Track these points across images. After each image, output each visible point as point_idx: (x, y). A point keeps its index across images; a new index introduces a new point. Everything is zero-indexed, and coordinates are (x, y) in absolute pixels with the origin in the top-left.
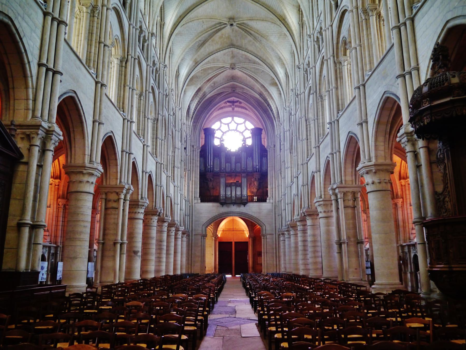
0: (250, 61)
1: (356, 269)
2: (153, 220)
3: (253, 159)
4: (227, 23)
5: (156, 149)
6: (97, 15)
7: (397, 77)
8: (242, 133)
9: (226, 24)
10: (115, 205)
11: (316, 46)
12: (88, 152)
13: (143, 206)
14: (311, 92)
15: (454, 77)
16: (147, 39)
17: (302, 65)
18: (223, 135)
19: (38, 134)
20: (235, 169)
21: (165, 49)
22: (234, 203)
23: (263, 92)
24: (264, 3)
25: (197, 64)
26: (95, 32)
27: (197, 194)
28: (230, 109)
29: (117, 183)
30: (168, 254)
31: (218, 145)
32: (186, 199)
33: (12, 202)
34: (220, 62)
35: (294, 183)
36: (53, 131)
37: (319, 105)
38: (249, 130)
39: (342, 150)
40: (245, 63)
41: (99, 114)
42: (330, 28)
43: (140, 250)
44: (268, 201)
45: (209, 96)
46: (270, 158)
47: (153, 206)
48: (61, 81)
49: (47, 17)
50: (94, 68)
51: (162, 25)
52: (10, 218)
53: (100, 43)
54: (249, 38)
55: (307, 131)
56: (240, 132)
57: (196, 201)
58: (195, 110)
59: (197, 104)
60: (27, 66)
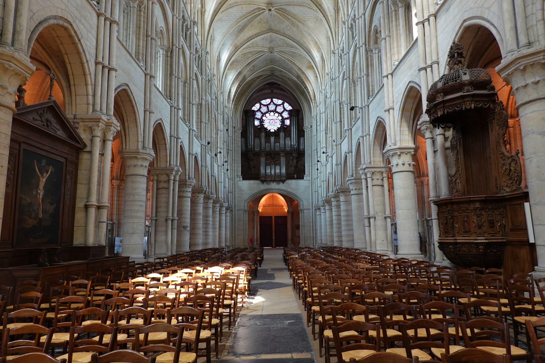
0: (288, 45)
1: (383, 241)
2: (199, 198)
3: (291, 138)
5: (201, 132)
6: (143, 10)
7: (420, 70)
8: (280, 114)
9: (264, 9)
10: (165, 185)
11: (350, 33)
12: (141, 139)
13: (191, 185)
14: (345, 77)
15: (465, 74)
16: (189, 27)
17: (337, 50)
18: (262, 116)
19: (98, 126)
20: (274, 149)
21: (206, 36)
22: (274, 181)
23: (301, 75)
25: (236, 48)
26: (142, 26)
27: (239, 172)
28: (269, 91)
30: (214, 228)
31: (259, 126)
32: (229, 177)
33: (79, 186)
34: (259, 47)
35: (329, 162)
36: (112, 123)
37: (352, 90)
38: (287, 111)
39: (371, 133)
40: (283, 47)
41: (150, 104)
42: (363, 16)
43: (189, 225)
44: (305, 178)
45: (248, 79)
46: (307, 138)
47: (199, 185)
48: (116, 77)
49: (100, 17)
50: (143, 61)
51: (203, 13)
52: (78, 200)
53: (147, 36)
55: (341, 114)
57: (238, 179)
58: (236, 93)
59: (238, 87)
60: (86, 65)
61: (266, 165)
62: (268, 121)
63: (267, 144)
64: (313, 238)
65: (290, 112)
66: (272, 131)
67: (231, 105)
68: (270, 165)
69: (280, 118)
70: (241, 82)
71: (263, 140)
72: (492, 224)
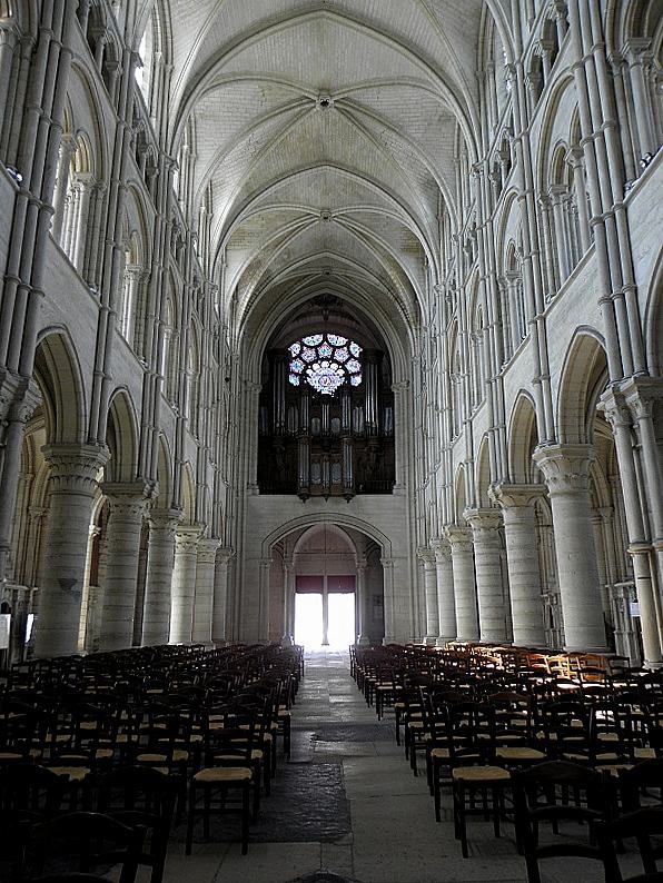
2: (131, 509)
4: (316, 98)
5: (145, 343)
8: (342, 365)
18: (306, 368)
21: (172, 124)
22: (327, 496)
24: (396, 35)
27: (252, 477)
28: (321, 318)
37: (541, 221)
40: (350, 205)
44: (394, 491)
54: (362, 138)
55: (499, 307)
57: (251, 491)
64: (414, 624)
65: (362, 359)
67: (237, 331)
69: (341, 372)
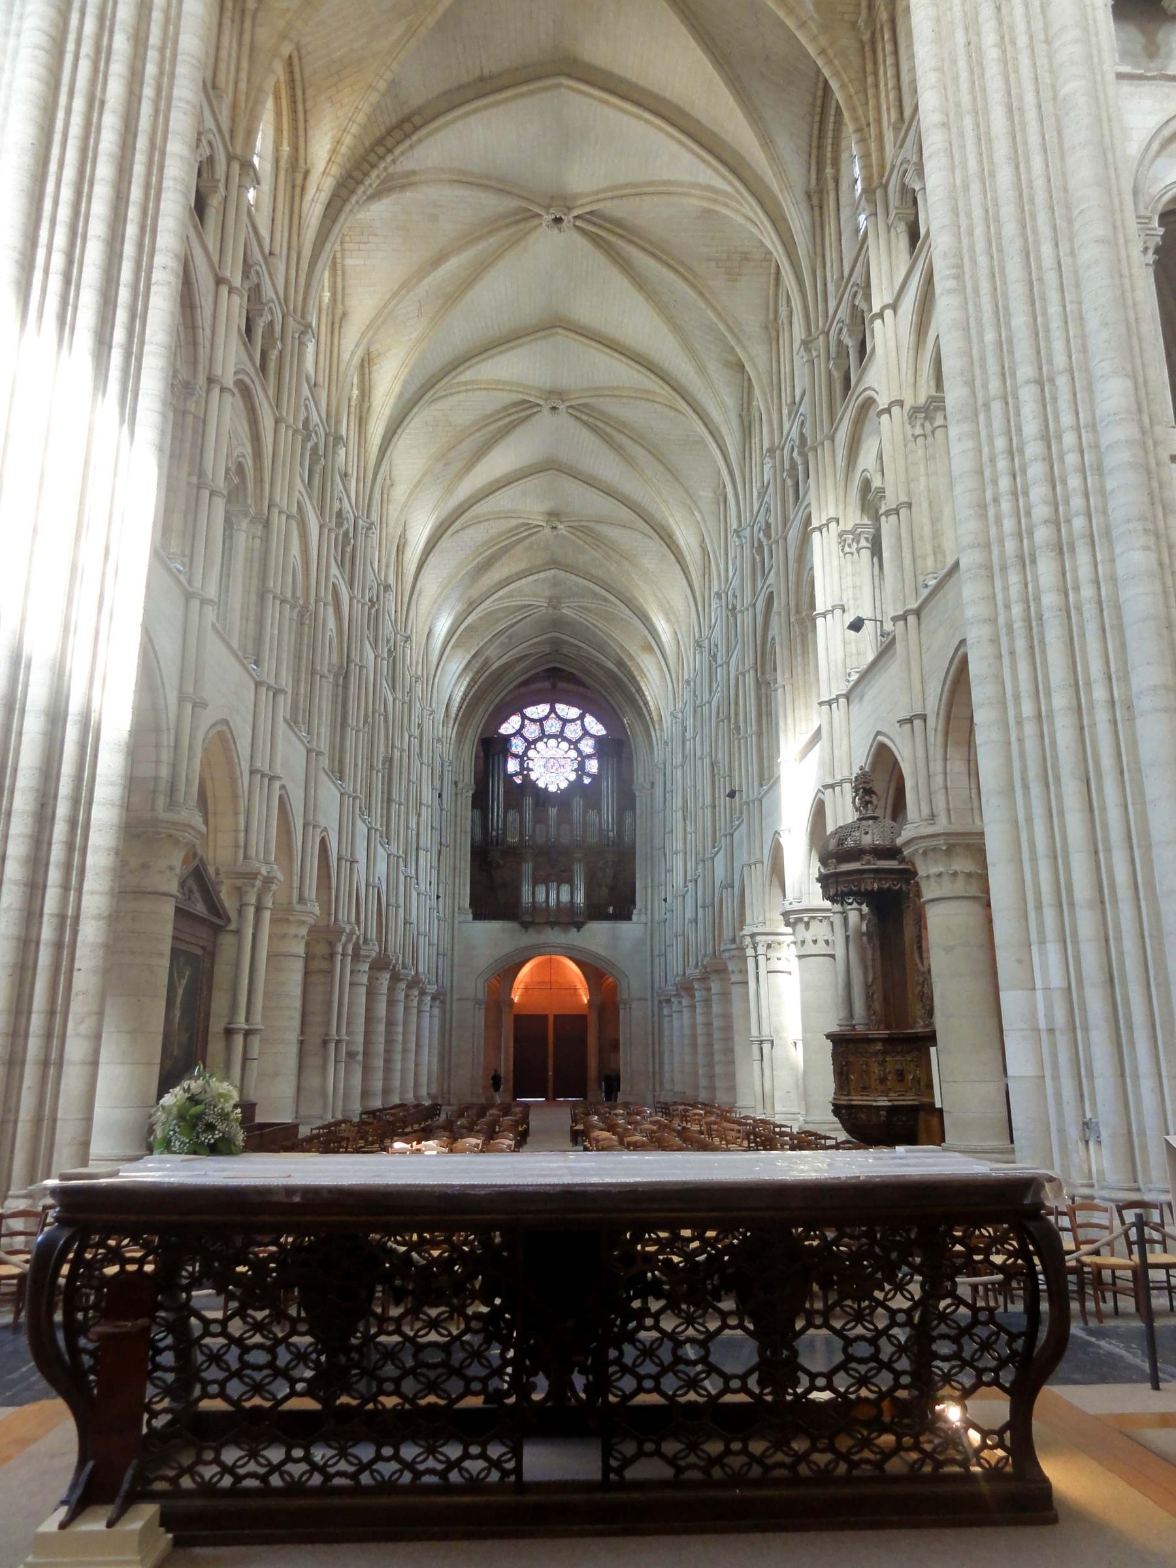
0: (595, 595)
8: (574, 744)
10: (324, 965)
18: (528, 748)
21: (406, 599)
22: (553, 924)
25: (472, 606)
29: (329, 920)
32: (441, 915)
33: (216, 995)
39: (765, 860)
41: (315, 810)
44: (634, 917)
53: (313, 672)
56: (569, 741)
57: (462, 918)
61: (535, 882)
62: (542, 762)
63: (538, 826)
65: (599, 740)
66: (552, 788)
67: (451, 732)
68: (546, 881)
69: (573, 754)
70: (477, 673)
71: (528, 815)
72: (901, 1075)
